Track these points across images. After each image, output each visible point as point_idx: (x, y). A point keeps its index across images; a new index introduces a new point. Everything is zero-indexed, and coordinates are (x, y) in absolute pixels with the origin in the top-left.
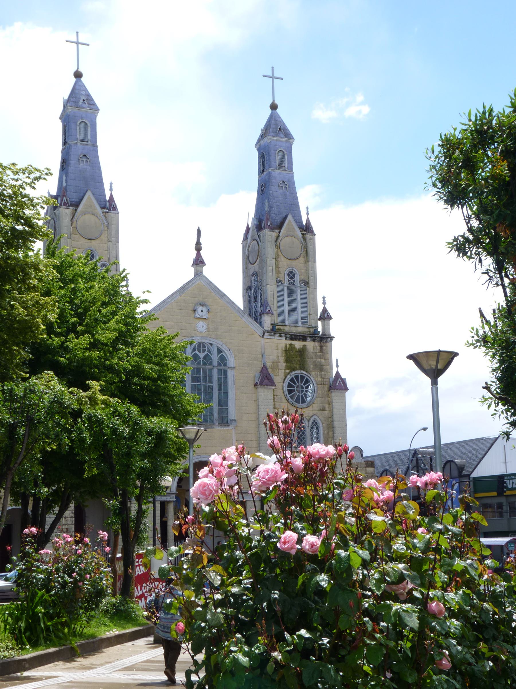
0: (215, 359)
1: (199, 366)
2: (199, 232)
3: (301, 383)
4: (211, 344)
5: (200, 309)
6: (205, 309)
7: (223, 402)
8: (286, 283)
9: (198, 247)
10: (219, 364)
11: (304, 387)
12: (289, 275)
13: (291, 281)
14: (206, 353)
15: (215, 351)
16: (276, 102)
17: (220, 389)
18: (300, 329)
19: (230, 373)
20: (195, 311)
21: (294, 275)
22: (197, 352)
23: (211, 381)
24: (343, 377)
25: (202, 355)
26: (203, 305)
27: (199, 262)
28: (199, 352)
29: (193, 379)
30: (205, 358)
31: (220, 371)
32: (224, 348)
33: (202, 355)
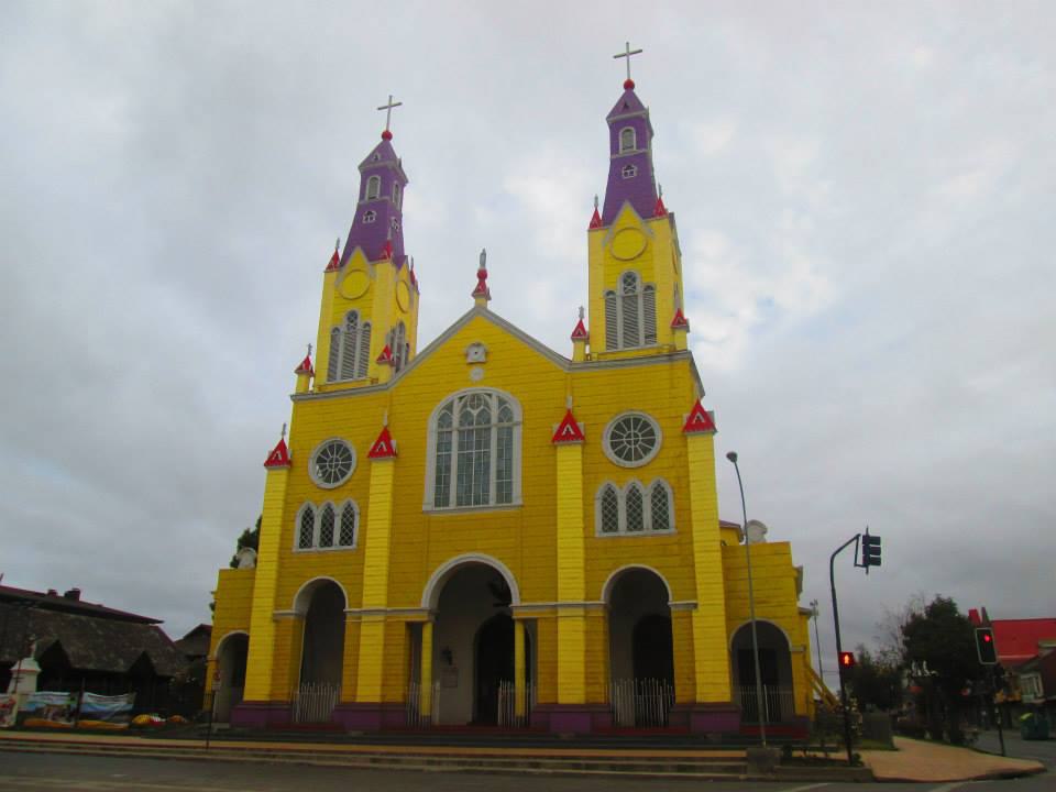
0: (494, 413)
1: (471, 427)
2: (484, 255)
3: (635, 428)
4: (490, 395)
5: (476, 350)
6: (480, 350)
7: (505, 473)
8: (619, 292)
9: (482, 275)
10: (500, 420)
11: (640, 434)
12: (625, 281)
13: (630, 287)
14: (482, 407)
15: (494, 403)
16: (632, 79)
17: (500, 456)
18: (642, 349)
19: (517, 432)
20: (467, 355)
21: (634, 280)
22: (469, 409)
23: (488, 445)
24: (706, 410)
25: (475, 413)
26: (478, 345)
27: (481, 291)
28: (473, 407)
29: (461, 447)
30: (479, 415)
31: (500, 430)
32: (505, 394)
33: (475, 413)
